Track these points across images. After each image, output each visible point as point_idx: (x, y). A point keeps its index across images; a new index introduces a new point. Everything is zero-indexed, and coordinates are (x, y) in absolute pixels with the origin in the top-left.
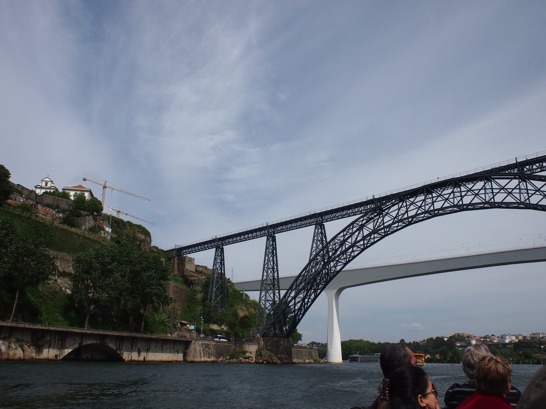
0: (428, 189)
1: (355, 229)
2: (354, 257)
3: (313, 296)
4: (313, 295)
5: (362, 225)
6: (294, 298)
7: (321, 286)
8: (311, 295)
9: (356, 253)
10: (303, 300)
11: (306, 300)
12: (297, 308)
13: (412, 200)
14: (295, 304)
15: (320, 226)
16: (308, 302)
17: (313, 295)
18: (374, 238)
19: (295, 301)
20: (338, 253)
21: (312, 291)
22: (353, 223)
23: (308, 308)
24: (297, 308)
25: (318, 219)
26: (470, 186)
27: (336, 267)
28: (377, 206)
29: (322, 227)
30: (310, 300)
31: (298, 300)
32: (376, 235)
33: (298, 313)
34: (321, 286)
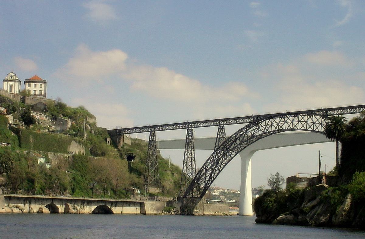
0: (282, 115)
1: (242, 133)
2: (242, 150)
3: (217, 172)
4: (217, 171)
5: (247, 131)
6: (205, 174)
7: (222, 166)
8: (216, 171)
9: (242, 148)
10: (211, 174)
11: (213, 175)
12: (207, 179)
13: (274, 119)
14: (205, 178)
15: (221, 128)
16: (214, 175)
17: (217, 171)
18: (252, 140)
19: (205, 176)
20: (232, 147)
21: (217, 169)
22: (241, 130)
23: (214, 179)
24: (207, 179)
25: (221, 123)
26: (303, 117)
27: (230, 155)
28: (256, 120)
29: (223, 128)
30: (215, 175)
31: (207, 174)
32: (253, 139)
33: (207, 183)
34: (222, 166)
